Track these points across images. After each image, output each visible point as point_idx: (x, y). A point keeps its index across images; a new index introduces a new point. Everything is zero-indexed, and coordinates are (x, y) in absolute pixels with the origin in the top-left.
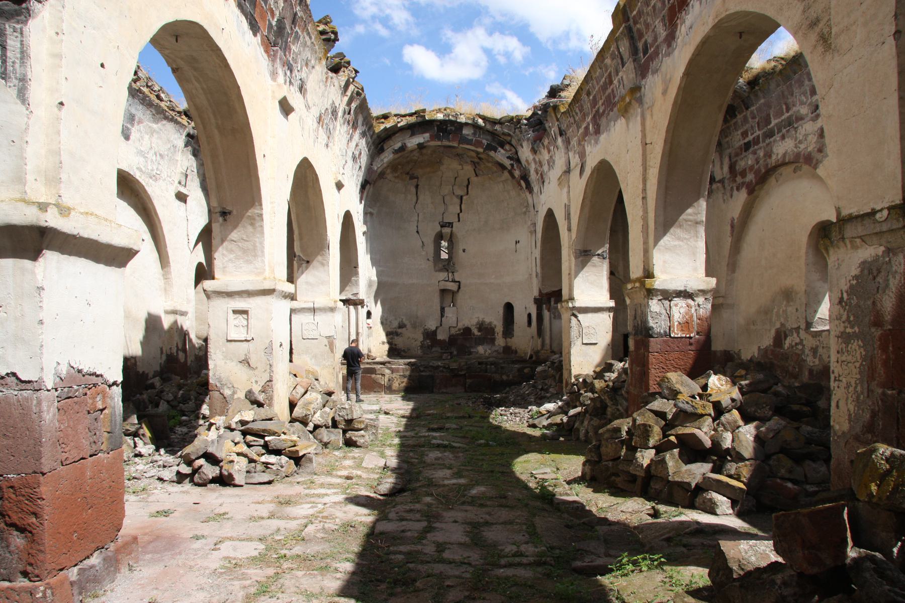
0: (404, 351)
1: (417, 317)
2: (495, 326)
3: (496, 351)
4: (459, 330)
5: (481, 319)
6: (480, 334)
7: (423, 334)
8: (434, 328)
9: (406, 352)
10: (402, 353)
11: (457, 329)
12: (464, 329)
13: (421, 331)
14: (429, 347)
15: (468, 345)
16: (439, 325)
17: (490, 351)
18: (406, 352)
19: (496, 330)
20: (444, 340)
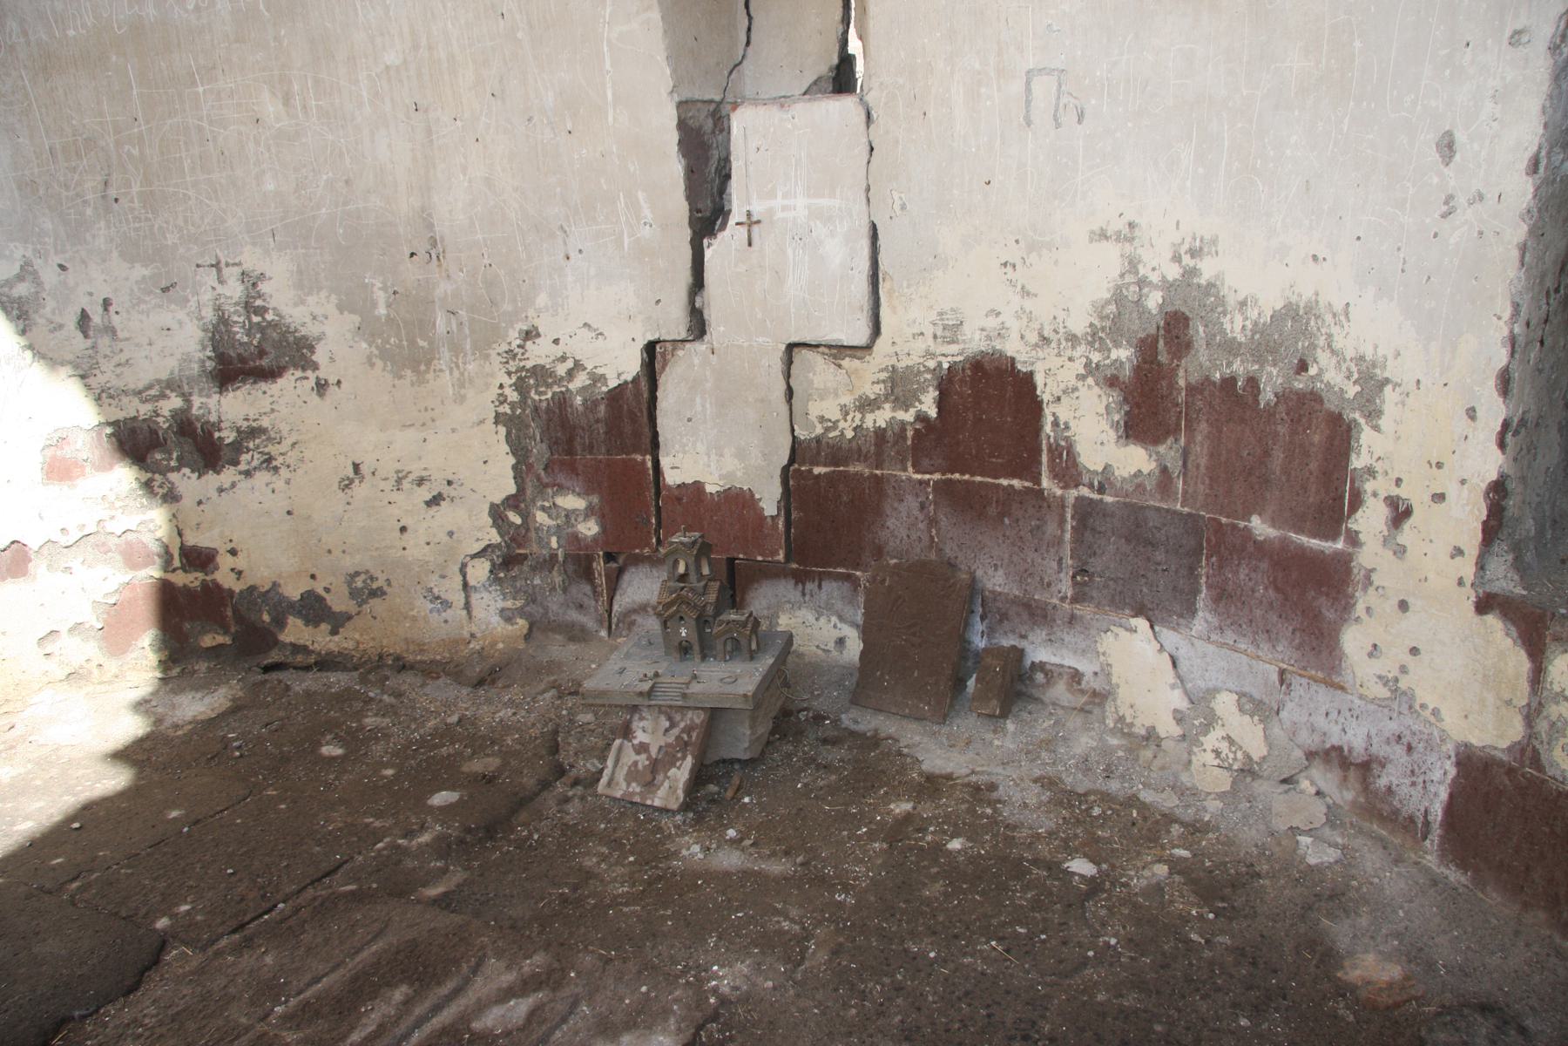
0: (313, 608)
1: (434, 250)
2: (1372, 384)
3: (1336, 757)
4: (899, 386)
5: (1160, 266)
6: (1134, 461)
7: (513, 425)
8: (624, 365)
9: (338, 622)
10: (295, 631)
11: (868, 376)
12: (947, 384)
13: (483, 402)
14: (579, 563)
15: (996, 581)
16: (674, 323)
17: (1253, 740)
18: (338, 622)
19: (1369, 448)
20: (739, 501)
